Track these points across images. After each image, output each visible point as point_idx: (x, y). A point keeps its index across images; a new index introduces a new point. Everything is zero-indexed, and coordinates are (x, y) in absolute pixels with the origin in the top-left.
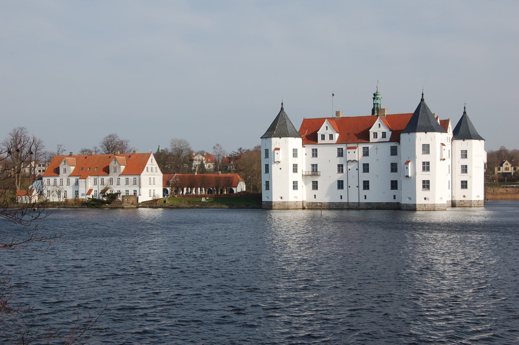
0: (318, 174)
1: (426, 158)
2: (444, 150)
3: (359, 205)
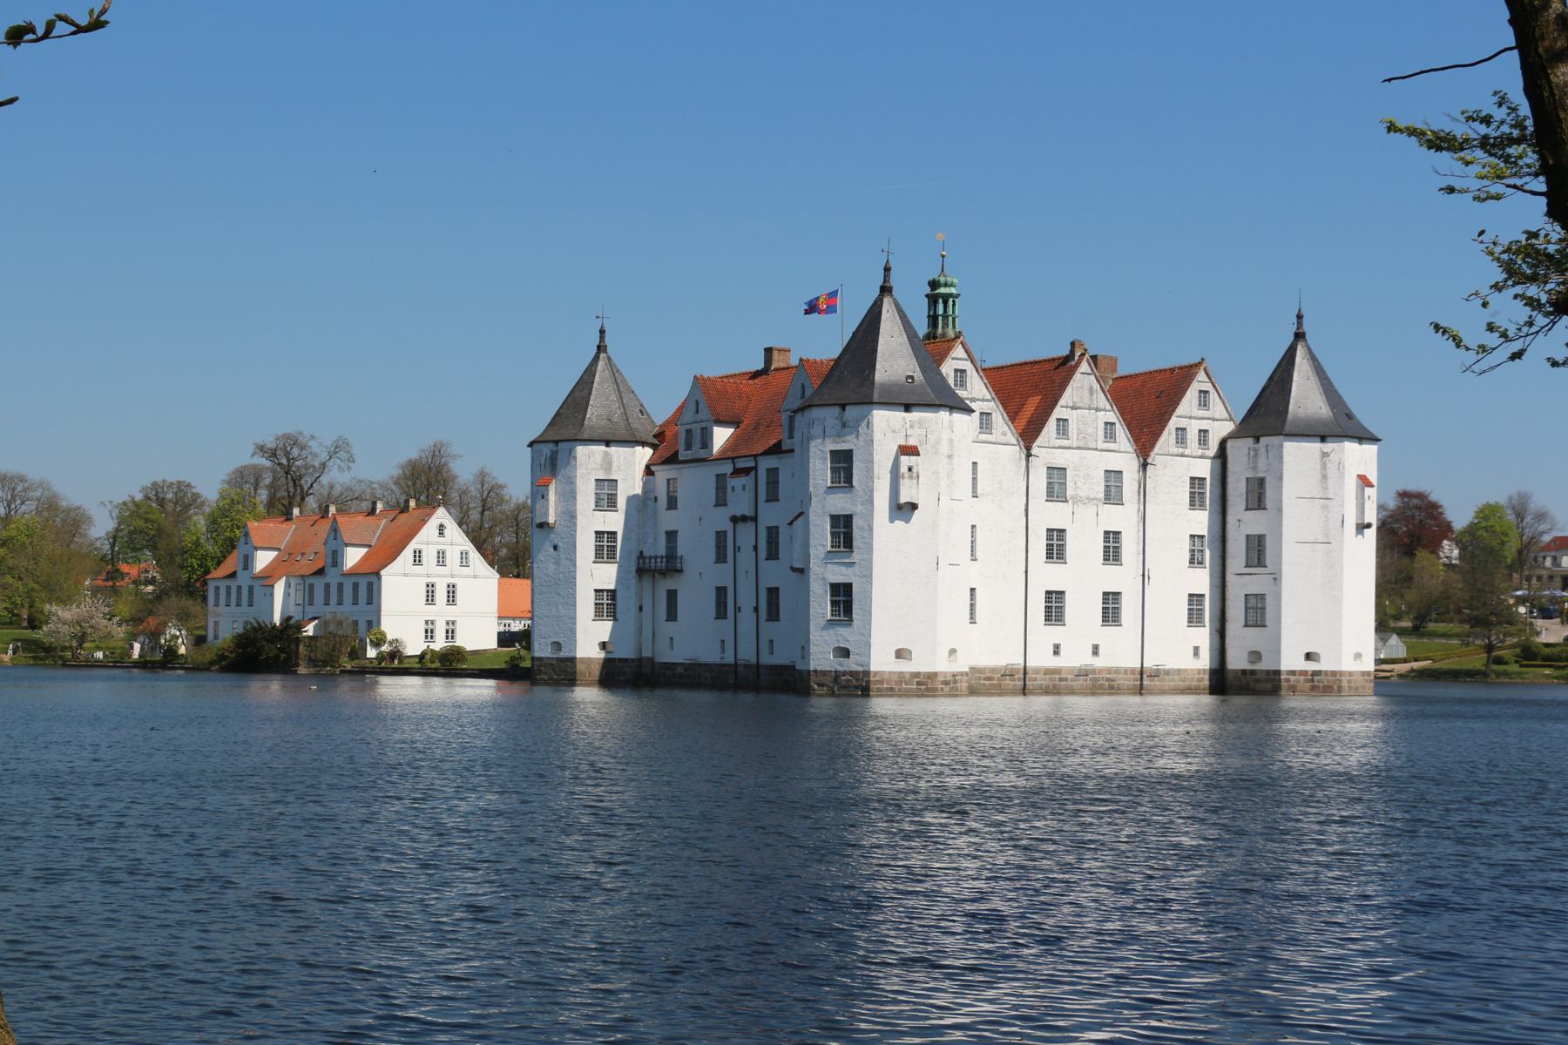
0: (679, 566)
1: (840, 503)
2: (910, 469)
3: (758, 674)
